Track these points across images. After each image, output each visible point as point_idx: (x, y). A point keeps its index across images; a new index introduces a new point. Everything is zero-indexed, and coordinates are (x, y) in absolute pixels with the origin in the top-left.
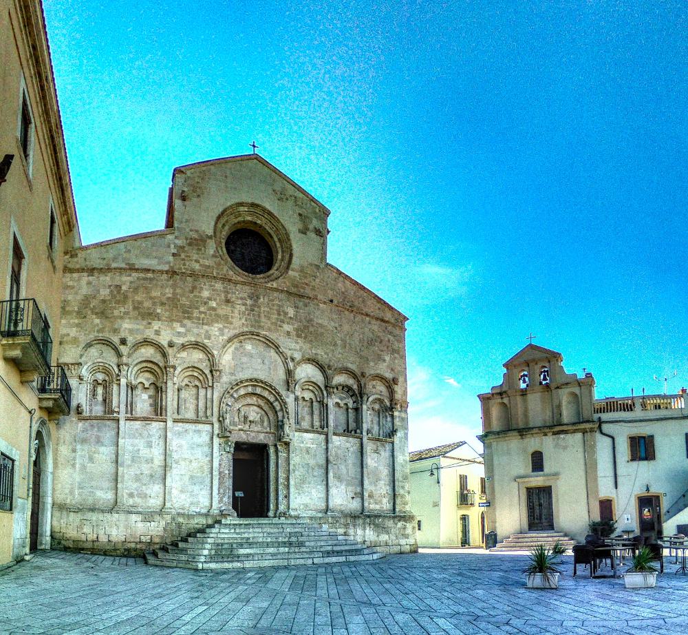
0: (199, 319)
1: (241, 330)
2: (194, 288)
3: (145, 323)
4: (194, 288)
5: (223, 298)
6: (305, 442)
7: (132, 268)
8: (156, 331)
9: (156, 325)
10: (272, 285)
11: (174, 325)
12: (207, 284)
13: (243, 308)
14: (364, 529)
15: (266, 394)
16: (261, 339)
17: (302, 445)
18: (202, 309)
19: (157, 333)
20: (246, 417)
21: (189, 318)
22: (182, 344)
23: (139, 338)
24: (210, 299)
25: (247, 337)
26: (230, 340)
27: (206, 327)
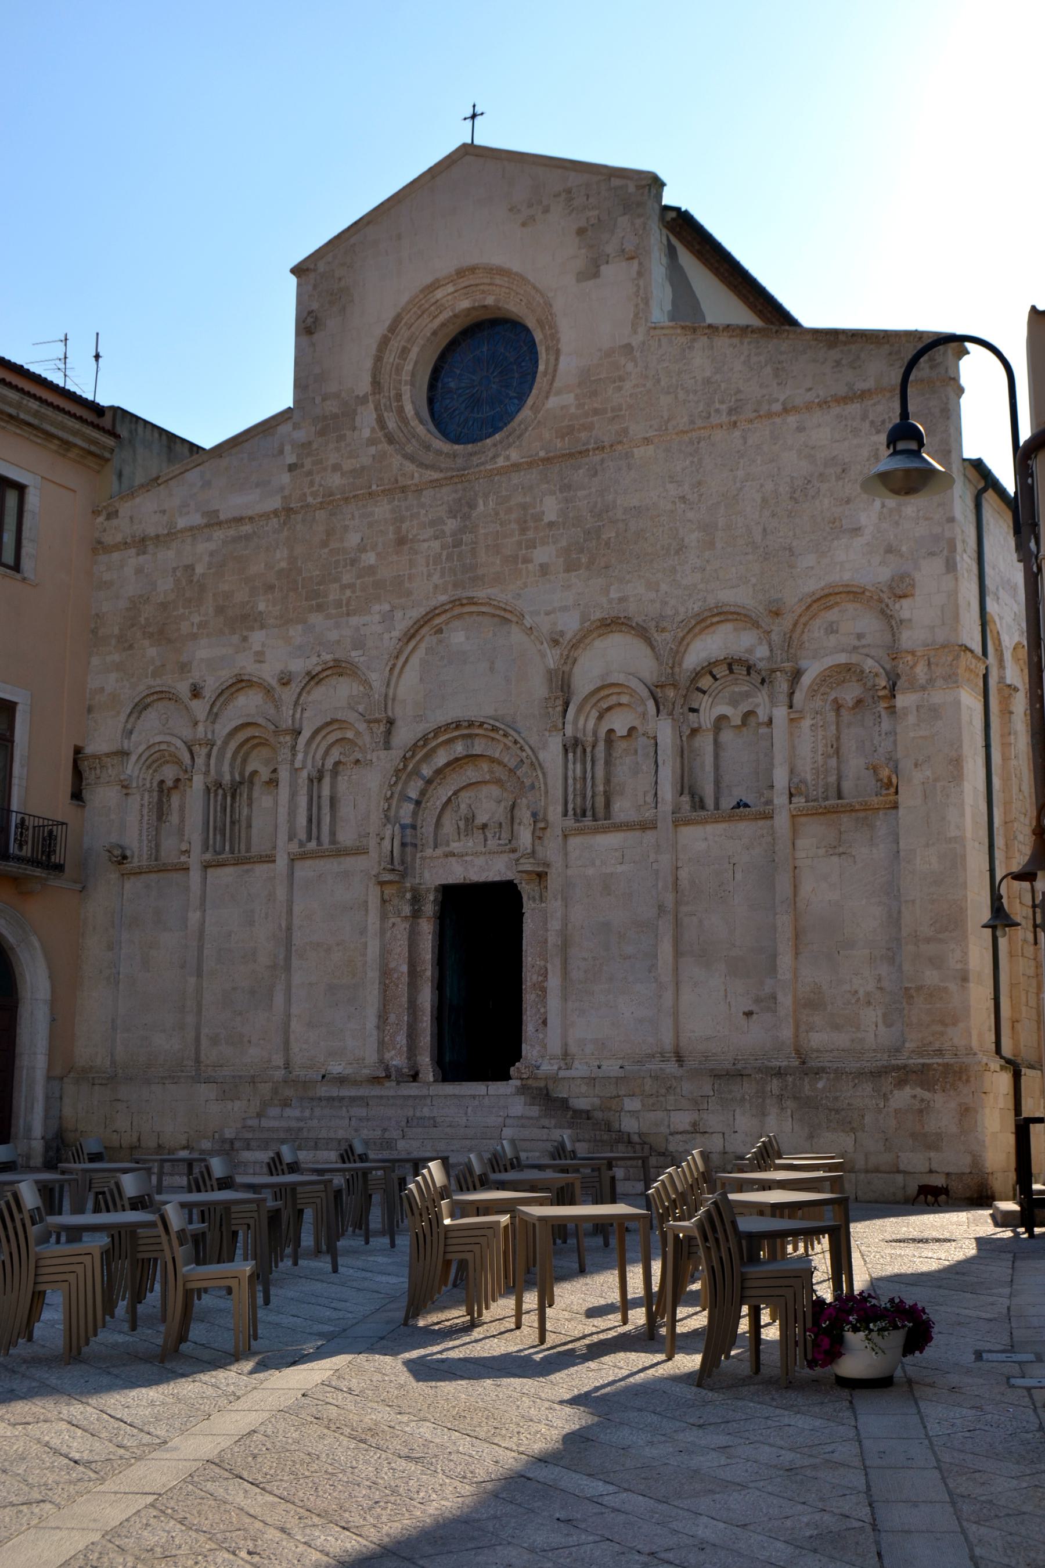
0: (338, 604)
1: (433, 603)
2: (330, 533)
3: (235, 639)
4: (330, 533)
5: (391, 536)
6: (598, 862)
7: (214, 522)
8: (257, 653)
9: (257, 638)
10: (508, 458)
11: (291, 633)
12: (357, 514)
13: (436, 545)
14: (762, 1113)
15: (441, 758)
16: (484, 609)
17: (590, 871)
18: (347, 578)
19: (260, 658)
20: (470, 820)
21: (320, 608)
22: (308, 673)
23: (226, 675)
24: (362, 549)
25: (448, 615)
26: (410, 636)
27: (354, 620)
